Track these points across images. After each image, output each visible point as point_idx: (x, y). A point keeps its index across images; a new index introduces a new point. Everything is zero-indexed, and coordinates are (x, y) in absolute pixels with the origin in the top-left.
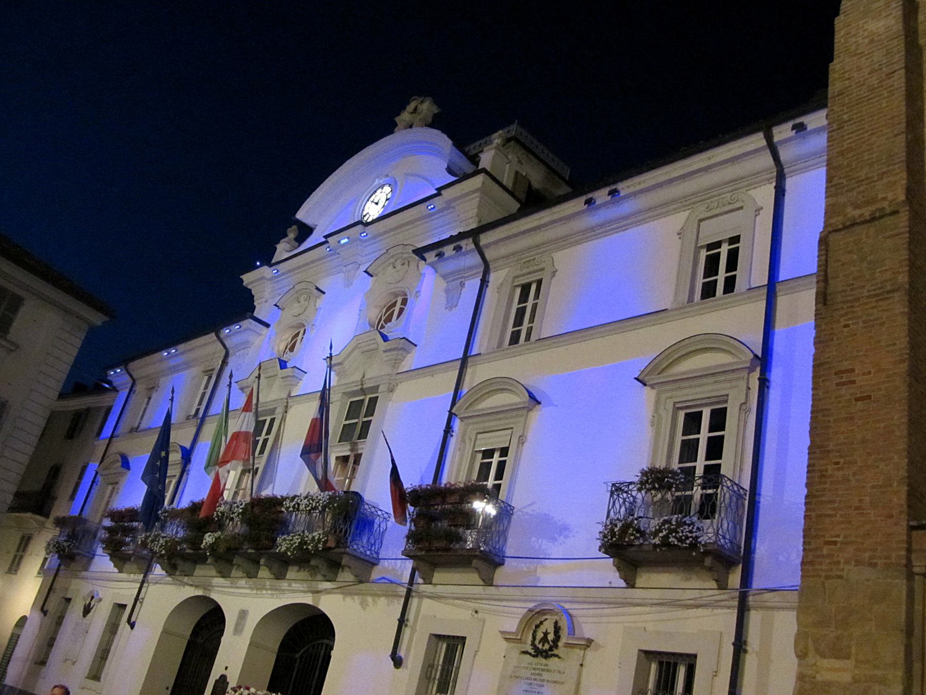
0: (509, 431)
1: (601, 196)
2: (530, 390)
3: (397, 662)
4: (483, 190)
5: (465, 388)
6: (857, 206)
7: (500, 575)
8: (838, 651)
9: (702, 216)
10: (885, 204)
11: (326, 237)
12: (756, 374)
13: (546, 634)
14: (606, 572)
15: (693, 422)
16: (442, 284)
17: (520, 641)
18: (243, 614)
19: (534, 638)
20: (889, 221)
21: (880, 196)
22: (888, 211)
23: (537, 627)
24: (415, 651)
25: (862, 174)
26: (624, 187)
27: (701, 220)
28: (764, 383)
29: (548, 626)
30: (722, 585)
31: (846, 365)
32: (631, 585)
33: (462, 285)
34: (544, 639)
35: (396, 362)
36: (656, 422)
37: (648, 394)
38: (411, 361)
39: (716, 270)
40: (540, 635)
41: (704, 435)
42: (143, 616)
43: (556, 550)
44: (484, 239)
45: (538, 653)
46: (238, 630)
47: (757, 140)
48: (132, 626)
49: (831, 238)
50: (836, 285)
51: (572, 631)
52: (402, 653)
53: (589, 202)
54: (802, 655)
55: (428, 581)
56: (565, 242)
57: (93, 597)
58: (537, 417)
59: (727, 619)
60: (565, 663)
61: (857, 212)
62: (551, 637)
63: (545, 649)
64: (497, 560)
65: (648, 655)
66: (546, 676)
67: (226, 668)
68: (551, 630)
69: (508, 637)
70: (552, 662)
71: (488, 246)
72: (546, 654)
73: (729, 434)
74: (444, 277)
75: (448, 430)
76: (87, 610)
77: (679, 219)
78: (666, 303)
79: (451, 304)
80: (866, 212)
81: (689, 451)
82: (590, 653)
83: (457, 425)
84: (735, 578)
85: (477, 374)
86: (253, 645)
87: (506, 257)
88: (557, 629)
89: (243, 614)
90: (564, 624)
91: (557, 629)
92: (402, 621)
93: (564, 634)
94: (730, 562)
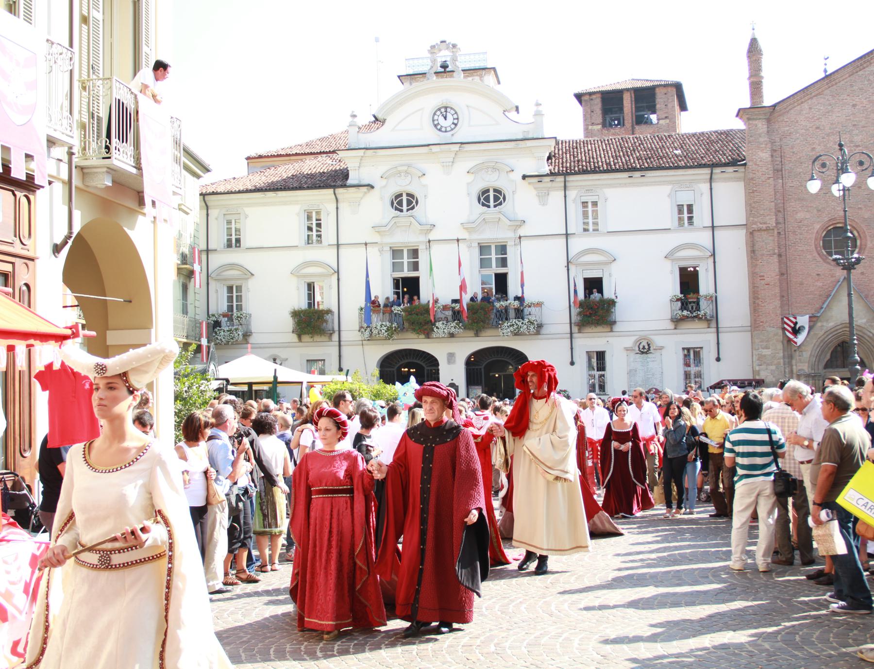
3: (572, 363)
7: (616, 328)
25: (762, 212)
28: (714, 262)
29: (644, 343)
32: (675, 329)
34: (644, 348)
40: (641, 347)
45: (643, 353)
59: (712, 337)
62: (647, 347)
70: (649, 355)
72: (646, 353)
75: (568, 270)
77: (667, 189)
80: (764, 226)
82: (663, 352)
84: (714, 324)
91: (649, 345)
92: (572, 349)
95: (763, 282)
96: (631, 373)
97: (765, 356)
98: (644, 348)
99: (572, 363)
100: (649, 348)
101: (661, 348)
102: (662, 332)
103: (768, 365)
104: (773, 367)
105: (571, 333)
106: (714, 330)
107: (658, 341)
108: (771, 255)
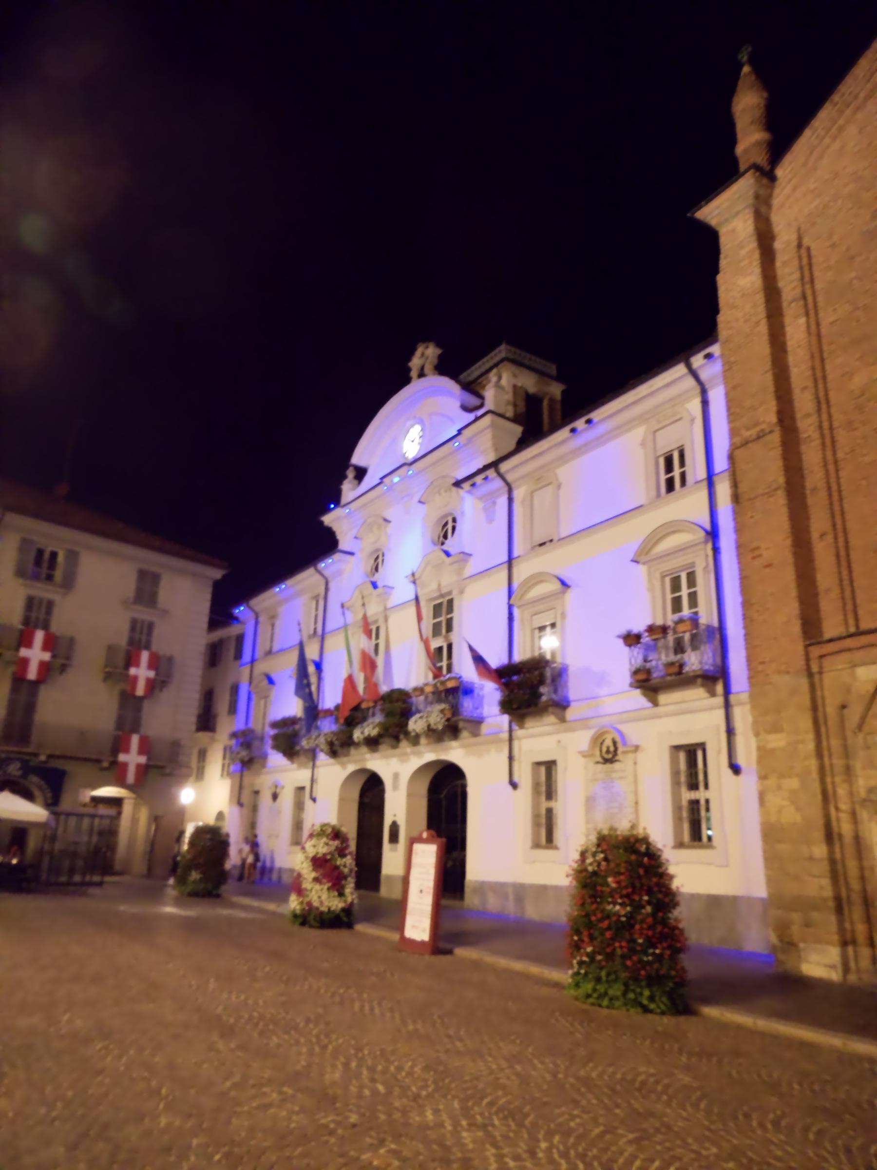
0: (552, 612)
1: (580, 424)
2: (562, 577)
3: (514, 785)
4: (493, 425)
5: (516, 583)
6: (748, 429)
7: (570, 714)
8: (776, 729)
9: (657, 427)
10: (764, 426)
11: (382, 478)
12: (710, 546)
13: (608, 748)
14: (637, 698)
15: (676, 585)
16: (480, 505)
17: (592, 755)
18: (396, 776)
19: (601, 751)
20: (769, 438)
21: (762, 419)
22: (767, 431)
23: (602, 744)
24: (524, 775)
26: (597, 415)
27: (655, 432)
29: (608, 742)
30: (713, 694)
31: (755, 545)
33: (494, 503)
34: (608, 752)
35: (459, 572)
36: (651, 589)
37: (642, 569)
38: (470, 568)
39: (671, 473)
40: (604, 749)
41: (684, 592)
42: (320, 791)
43: (603, 691)
44: (504, 467)
45: (606, 761)
46: (395, 787)
47: (680, 369)
48: (314, 800)
49: (738, 453)
50: (743, 487)
51: (624, 743)
52: (516, 779)
53: (573, 430)
54: (757, 734)
55: (521, 726)
56: (563, 460)
57: (276, 787)
58: (570, 595)
59: (719, 715)
60: (625, 764)
61: (748, 433)
62: (612, 749)
63: (610, 757)
64: (565, 704)
65: (677, 748)
66: (614, 775)
67: (395, 815)
68: (611, 744)
69: (584, 755)
70: (616, 766)
71: (508, 471)
73: (700, 588)
74: (480, 498)
76: (275, 797)
77: (639, 433)
78: (642, 500)
79: (490, 519)
80: (753, 432)
81: (677, 605)
82: (640, 756)
83: (516, 612)
84: (720, 688)
85: (522, 572)
86: (410, 795)
87: (522, 477)
88: (615, 743)
89: (396, 776)
90: (618, 739)
91: (615, 743)
92: (511, 758)
93: (619, 745)
94: (716, 677)
95: (758, 563)
96: (590, 802)
97: (773, 751)
98: (608, 748)
99: (514, 785)
100: (616, 749)
101: (637, 748)
102: (635, 717)
103: (782, 776)
104: (793, 783)
105: (511, 731)
106: (719, 700)
107: (633, 732)
108: (770, 494)
